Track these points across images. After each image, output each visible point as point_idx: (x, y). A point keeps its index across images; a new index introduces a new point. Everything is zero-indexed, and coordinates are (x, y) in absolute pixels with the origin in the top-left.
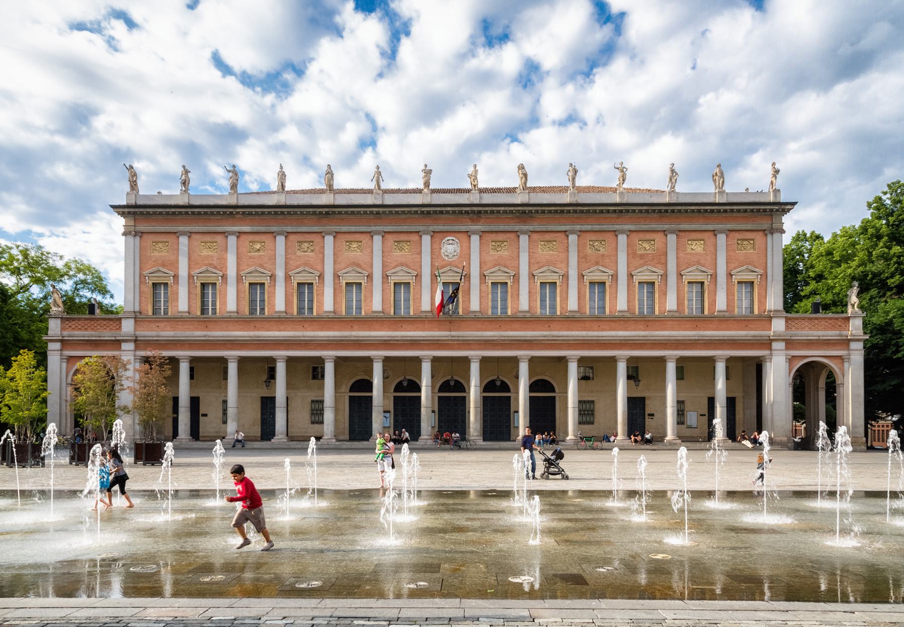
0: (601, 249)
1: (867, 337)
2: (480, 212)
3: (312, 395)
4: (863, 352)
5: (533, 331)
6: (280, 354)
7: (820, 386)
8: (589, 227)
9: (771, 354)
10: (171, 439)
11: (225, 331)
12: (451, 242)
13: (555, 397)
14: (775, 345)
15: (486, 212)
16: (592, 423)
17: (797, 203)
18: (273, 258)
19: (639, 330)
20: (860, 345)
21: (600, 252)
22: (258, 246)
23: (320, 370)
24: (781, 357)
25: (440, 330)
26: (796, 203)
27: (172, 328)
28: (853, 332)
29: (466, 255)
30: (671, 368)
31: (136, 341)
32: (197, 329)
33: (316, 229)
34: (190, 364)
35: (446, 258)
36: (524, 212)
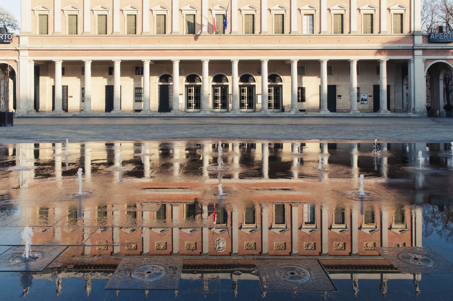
5: (270, 44)
7: (440, 78)
9: (414, 58)
14: (416, 52)
23: (141, 69)
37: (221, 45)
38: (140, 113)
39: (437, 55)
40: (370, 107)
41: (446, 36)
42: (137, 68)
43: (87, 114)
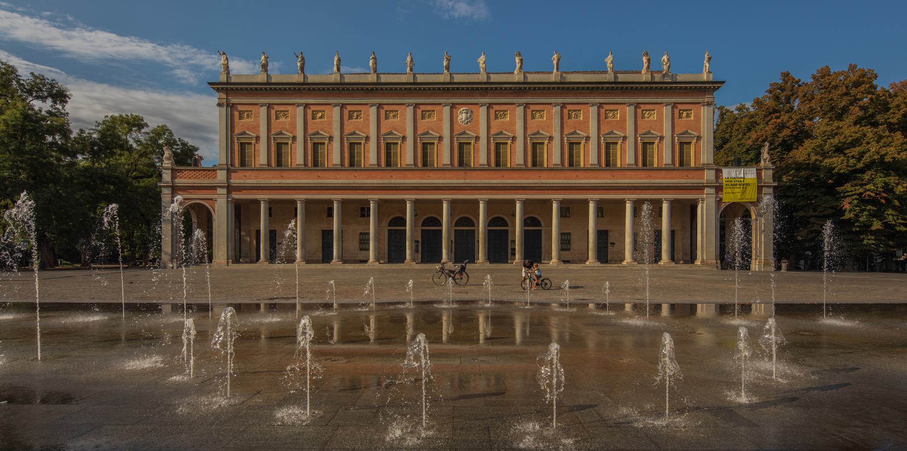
2: (487, 89)
3: (360, 229)
6: (336, 196)
10: (255, 261)
13: (541, 230)
15: (492, 88)
16: (569, 250)
18: (330, 124)
19: (607, 179)
20: (771, 190)
21: (577, 119)
22: (320, 115)
24: (712, 199)
25: (457, 179)
26: (724, 82)
28: (765, 180)
32: (274, 178)
33: (364, 101)
34: (269, 205)
36: (520, 89)
37: (467, 181)
38: (366, 265)
42: (363, 209)
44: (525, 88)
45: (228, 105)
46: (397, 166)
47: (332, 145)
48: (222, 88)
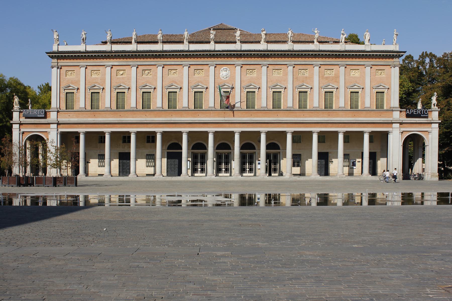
0: (305, 74)
1: (440, 122)
4: (438, 129)
5: (269, 117)
8: (299, 63)
11: (105, 118)
12: (225, 70)
17: (406, 51)
18: (129, 79)
19: (325, 117)
20: (437, 125)
21: (304, 76)
25: (219, 117)
27: (76, 116)
29: (233, 77)
30: (341, 137)
31: (58, 124)
32: (89, 117)
35: (223, 79)
37: (226, 119)
39: (411, 128)
40: (358, 171)
41: (419, 112)
43: (108, 177)
44: (268, 54)
45: (58, 68)
46: (176, 108)
47: (130, 94)
48: (55, 56)
